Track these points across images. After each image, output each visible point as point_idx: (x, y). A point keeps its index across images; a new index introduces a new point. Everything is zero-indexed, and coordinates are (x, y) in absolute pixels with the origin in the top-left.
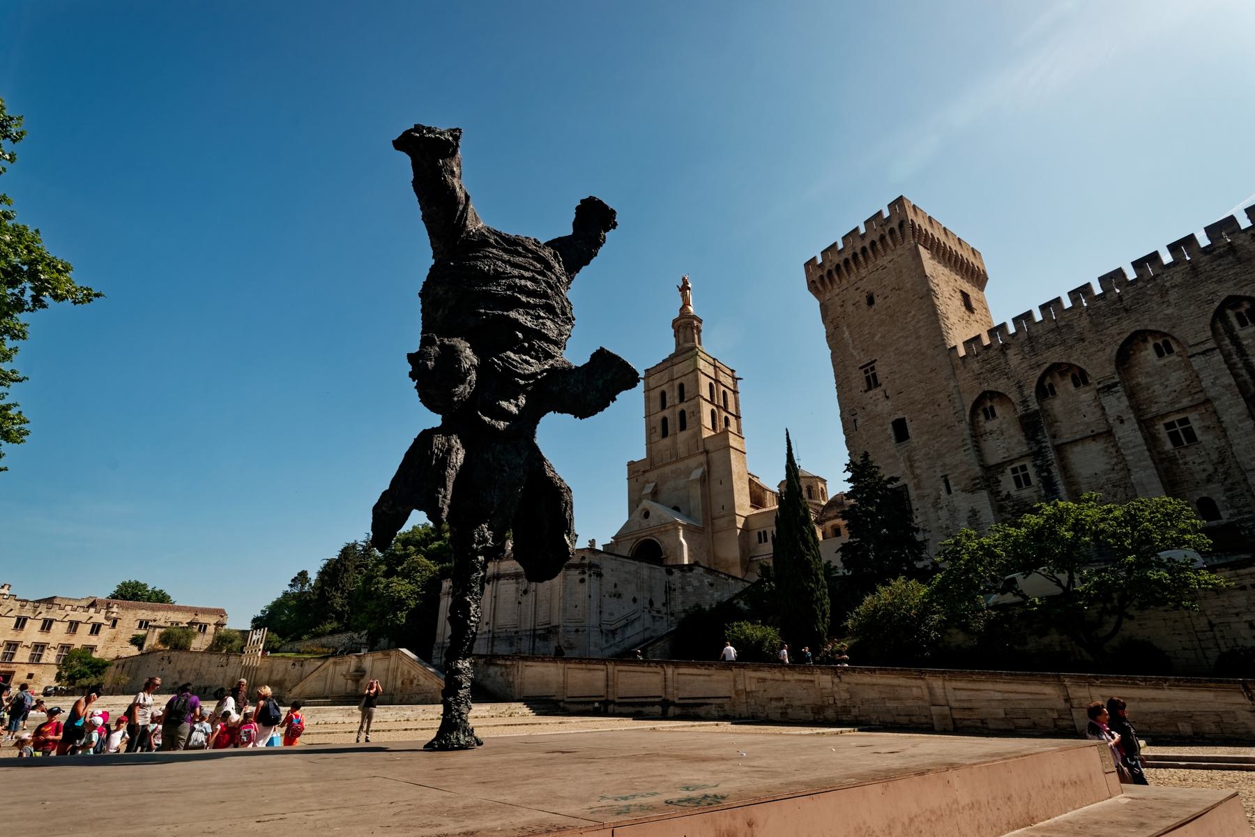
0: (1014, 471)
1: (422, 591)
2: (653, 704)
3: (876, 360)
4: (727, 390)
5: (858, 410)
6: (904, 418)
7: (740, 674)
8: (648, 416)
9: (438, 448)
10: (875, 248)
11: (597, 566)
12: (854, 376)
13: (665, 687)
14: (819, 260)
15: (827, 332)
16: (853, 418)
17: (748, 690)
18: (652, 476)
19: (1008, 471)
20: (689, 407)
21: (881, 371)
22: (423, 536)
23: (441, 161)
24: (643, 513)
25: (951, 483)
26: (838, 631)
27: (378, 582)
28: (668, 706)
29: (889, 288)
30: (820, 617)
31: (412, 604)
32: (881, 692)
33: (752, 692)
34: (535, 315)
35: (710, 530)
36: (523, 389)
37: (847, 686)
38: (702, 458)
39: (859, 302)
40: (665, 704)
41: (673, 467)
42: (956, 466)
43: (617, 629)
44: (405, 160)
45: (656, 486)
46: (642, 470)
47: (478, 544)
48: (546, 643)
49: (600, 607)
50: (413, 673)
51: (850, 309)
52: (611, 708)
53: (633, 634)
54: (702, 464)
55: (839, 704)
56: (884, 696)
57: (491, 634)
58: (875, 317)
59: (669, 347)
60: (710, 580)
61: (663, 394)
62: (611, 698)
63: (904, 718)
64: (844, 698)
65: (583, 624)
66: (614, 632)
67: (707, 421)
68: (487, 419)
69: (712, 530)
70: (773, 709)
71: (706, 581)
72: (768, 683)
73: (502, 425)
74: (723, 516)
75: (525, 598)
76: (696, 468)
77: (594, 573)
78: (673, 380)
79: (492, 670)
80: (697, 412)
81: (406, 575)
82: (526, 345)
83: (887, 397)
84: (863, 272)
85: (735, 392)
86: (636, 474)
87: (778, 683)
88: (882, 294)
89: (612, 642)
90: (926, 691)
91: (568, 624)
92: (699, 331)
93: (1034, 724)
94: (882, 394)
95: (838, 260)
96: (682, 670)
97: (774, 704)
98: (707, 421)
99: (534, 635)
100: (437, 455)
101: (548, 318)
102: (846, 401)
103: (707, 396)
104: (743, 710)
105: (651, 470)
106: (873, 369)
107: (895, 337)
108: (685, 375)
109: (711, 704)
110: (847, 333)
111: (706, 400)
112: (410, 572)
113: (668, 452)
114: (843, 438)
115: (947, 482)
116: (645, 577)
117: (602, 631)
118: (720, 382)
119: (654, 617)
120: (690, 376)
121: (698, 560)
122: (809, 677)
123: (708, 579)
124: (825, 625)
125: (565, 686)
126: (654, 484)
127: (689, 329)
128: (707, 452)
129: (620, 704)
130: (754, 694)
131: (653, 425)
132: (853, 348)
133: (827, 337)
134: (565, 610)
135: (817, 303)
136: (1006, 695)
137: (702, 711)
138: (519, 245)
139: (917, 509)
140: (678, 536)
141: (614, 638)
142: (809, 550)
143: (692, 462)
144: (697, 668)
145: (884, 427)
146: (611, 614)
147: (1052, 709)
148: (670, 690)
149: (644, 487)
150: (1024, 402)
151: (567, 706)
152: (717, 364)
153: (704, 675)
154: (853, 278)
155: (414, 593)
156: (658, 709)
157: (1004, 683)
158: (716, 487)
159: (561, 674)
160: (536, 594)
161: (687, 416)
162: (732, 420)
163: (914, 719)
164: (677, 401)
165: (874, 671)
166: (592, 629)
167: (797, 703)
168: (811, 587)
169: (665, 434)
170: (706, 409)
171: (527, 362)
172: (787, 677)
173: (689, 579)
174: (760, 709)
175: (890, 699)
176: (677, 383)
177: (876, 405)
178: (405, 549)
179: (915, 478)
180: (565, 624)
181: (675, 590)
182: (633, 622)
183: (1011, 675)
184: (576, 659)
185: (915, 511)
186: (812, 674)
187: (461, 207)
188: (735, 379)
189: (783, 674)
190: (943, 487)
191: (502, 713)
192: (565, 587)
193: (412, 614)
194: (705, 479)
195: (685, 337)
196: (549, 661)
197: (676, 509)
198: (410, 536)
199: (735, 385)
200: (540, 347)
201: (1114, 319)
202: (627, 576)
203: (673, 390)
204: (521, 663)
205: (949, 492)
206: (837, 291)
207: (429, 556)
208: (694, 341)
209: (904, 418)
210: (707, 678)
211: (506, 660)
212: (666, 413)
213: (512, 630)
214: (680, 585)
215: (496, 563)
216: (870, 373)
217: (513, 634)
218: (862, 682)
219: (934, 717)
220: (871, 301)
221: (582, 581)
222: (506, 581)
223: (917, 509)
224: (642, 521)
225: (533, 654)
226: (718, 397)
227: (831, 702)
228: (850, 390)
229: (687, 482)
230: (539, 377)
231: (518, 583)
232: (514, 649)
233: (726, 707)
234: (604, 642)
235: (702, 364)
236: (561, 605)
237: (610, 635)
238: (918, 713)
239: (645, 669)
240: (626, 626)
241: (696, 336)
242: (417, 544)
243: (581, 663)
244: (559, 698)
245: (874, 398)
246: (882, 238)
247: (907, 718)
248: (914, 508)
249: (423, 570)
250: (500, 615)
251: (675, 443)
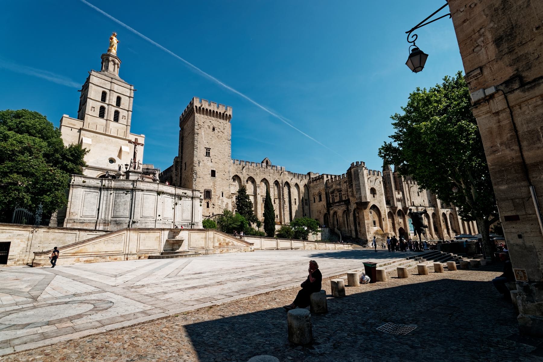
0: (236, 196)
5: (201, 160)
19: (235, 196)
25: (224, 194)
29: (220, 130)
42: (226, 190)
61: (104, 94)
106: (209, 150)
115: (223, 193)
150: (244, 182)
164: (115, 104)
177: (208, 162)
185: (212, 198)
190: (221, 194)
201: (262, 174)
205: (222, 196)
216: (208, 151)
220: (214, 129)
222: (167, 196)
246: (223, 114)
248: (212, 197)
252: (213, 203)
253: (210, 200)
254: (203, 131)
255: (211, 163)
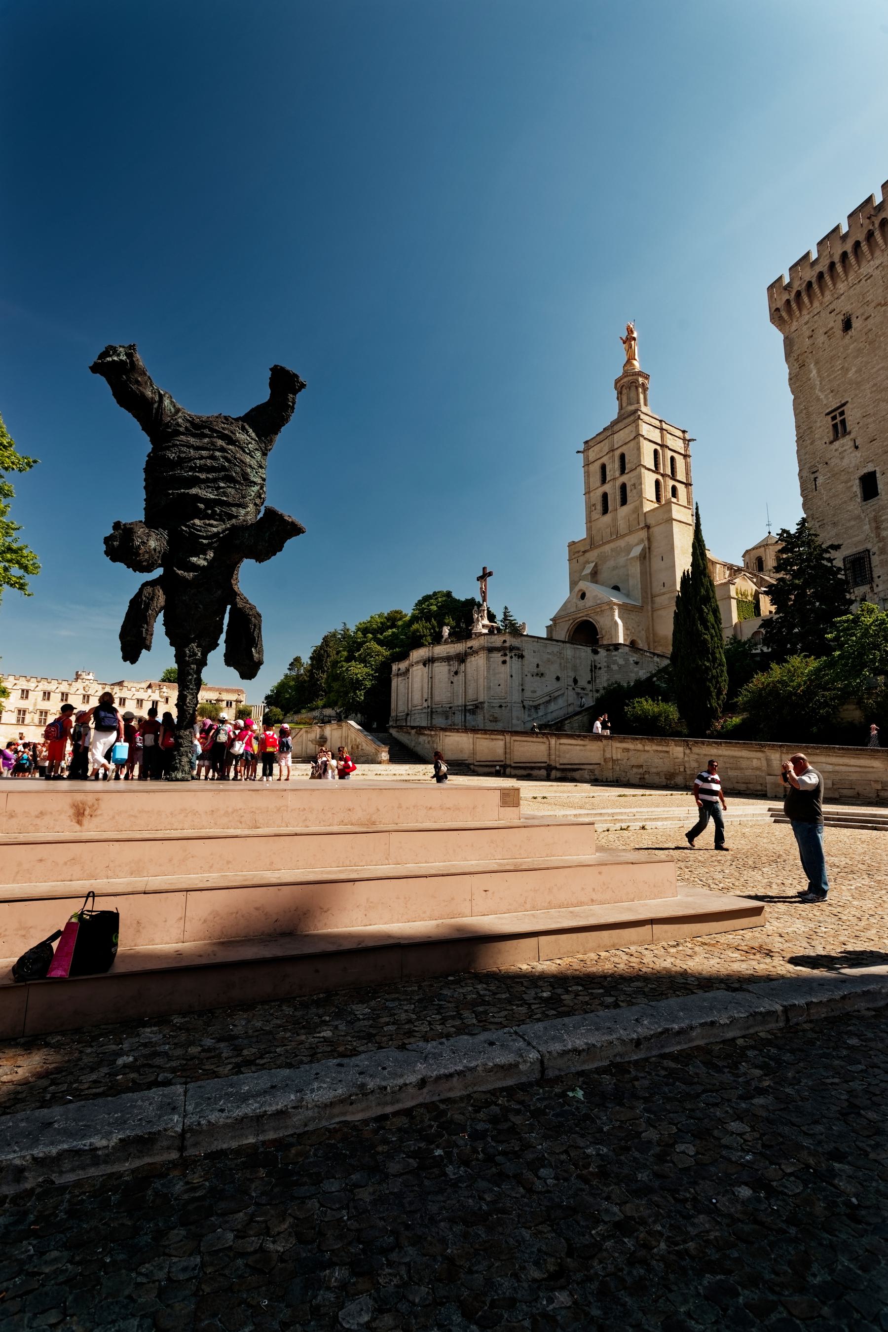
1: (375, 673)
2: (540, 768)
3: (847, 402)
4: (675, 455)
6: (875, 471)
7: (608, 745)
8: (587, 493)
9: (145, 597)
10: (859, 253)
11: (518, 649)
12: (818, 424)
13: (549, 755)
14: (786, 280)
15: (790, 374)
16: (813, 476)
17: (614, 758)
18: (593, 555)
20: (630, 480)
21: (852, 416)
22: (379, 625)
23: (124, 377)
24: (580, 594)
26: (730, 708)
27: (342, 666)
28: (551, 771)
29: (873, 305)
30: (714, 694)
31: (368, 684)
32: (725, 762)
33: (618, 760)
34: (215, 487)
35: (650, 608)
36: (209, 546)
37: (696, 756)
38: (643, 534)
39: (832, 328)
40: (549, 768)
41: (612, 545)
43: (539, 705)
44: (101, 381)
45: (596, 566)
46: (583, 549)
47: (190, 656)
48: (474, 716)
49: (522, 685)
50: (358, 740)
51: (821, 339)
52: (508, 770)
53: (556, 710)
54: (642, 540)
55: (688, 772)
56: (728, 765)
57: (429, 710)
58: (852, 346)
59: (612, 412)
60: (635, 659)
61: (603, 467)
62: (508, 763)
63: (743, 785)
64: (692, 766)
65: (505, 700)
66: (536, 708)
67: (649, 492)
68: (179, 572)
69: (652, 608)
70: (633, 777)
71: (631, 659)
72: (631, 753)
73: (190, 575)
74: (664, 594)
75: (456, 678)
76: (637, 544)
77: (515, 655)
78: (613, 450)
79: (422, 739)
80: (638, 485)
81: (363, 660)
82: (210, 512)
83: (857, 447)
84: (842, 287)
85: (685, 456)
86: (576, 555)
87: (639, 753)
88: (863, 314)
89: (535, 716)
90: (764, 763)
91: (492, 701)
92: (645, 389)
93: (858, 794)
94: (851, 444)
95: (809, 274)
96: (563, 741)
97: (635, 770)
98: (649, 492)
99: (465, 710)
100: (145, 601)
101: (229, 487)
102: (807, 456)
103: (650, 464)
104: (609, 775)
105: (591, 549)
106: (842, 413)
107: (875, 370)
108: (626, 444)
109: (585, 769)
110: (814, 372)
111: (649, 470)
112: (365, 657)
113: (608, 530)
114: (801, 500)
116: (569, 657)
117: (524, 707)
118: (667, 447)
119: (578, 694)
120: (632, 444)
121: (635, 638)
122: (664, 749)
123: (634, 658)
124: (720, 702)
125: (474, 753)
126: (594, 564)
127: (633, 389)
128: (648, 527)
129: (515, 768)
130: (619, 762)
131: (593, 502)
132: (820, 390)
133: (790, 379)
134: (489, 688)
135: (780, 337)
136: (837, 768)
137: (577, 775)
138: (205, 427)
139: (879, 577)
140: (613, 615)
141: (537, 713)
142: (707, 628)
143: (633, 539)
144: (575, 739)
145: (849, 484)
146: (534, 692)
147: (876, 781)
148: (553, 757)
149: (584, 567)
151: (476, 768)
152: (665, 426)
153: (580, 745)
154: (828, 297)
155: (369, 675)
156: (543, 772)
157: (837, 756)
158: (656, 564)
159: (471, 742)
160: (465, 675)
161: (628, 489)
162: (681, 489)
163: (751, 786)
164: (617, 473)
165: (721, 743)
166: (514, 705)
167: (654, 770)
168: (705, 665)
169: (605, 511)
170: (649, 480)
171: (212, 526)
172: (647, 748)
173: (614, 658)
174: (623, 774)
175: (731, 769)
176: (617, 453)
177: (842, 458)
178: (365, 637)
179: (880, 541)
180: (490, 701)
181: (600, 668)
182: (556, 698)
183: (843, 749)
184: (482, 730)
185: (876, 580)
186: (667, 746)
187: (156, 405)
188: (687, 442)
189: (644, 746)
191: (419, 772)
192: (488, 669)
193: (369, 693)
194: (645, 556)
195: (628, 398)
196: (462, 732)
197: (616, 588)
198: (368, 625)
199: (686, 448)
200: (222, 511)
202: (550, 657)
203: (614, 462)
204: (441, 733)
206: (806, 318)
207: (380, 643)
208: (638, 402)
209: (875, 471)
210: (582, 748)
211: (431, 730)
212: (607, 488)
213: (446, 705)
214: (605, 664)
215: (431, 648)
216: (839, 419)
217: (448, 709)
218: (709, 753)
219: (768, 786)
220: (847, 325)
221: (504, 662)
222: (439, 664)
223: (879, 577)
224: (579, 603)
225: (465, 726)
226: (664, 465)
227: (682, 770)
228: (812, 443)
229: (627, 560)
230: (221, 535)
231: (450, 665)
232: (450, 722)
233: (596, 773)
234: (526, 717)
235: (645, 429)
236: (486, 684)
237: (533, 710)
238: (755, 781)
239: (534, 739)
240: (549, 702)
241: (641, 396)
242: (374, 632)
243: (486, 734)
244: (470, 762)
245: (840, 450)
247: (745, 785)
248: (875, 575)
249: (376, 655)
250: (436, 692)
251: (615, 520)
252: (882, 595)
253: (872, 588)
254: (812, 366)
255: (858, 454)
